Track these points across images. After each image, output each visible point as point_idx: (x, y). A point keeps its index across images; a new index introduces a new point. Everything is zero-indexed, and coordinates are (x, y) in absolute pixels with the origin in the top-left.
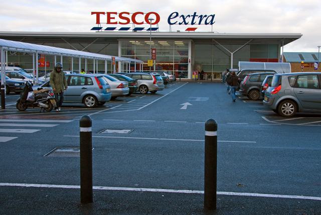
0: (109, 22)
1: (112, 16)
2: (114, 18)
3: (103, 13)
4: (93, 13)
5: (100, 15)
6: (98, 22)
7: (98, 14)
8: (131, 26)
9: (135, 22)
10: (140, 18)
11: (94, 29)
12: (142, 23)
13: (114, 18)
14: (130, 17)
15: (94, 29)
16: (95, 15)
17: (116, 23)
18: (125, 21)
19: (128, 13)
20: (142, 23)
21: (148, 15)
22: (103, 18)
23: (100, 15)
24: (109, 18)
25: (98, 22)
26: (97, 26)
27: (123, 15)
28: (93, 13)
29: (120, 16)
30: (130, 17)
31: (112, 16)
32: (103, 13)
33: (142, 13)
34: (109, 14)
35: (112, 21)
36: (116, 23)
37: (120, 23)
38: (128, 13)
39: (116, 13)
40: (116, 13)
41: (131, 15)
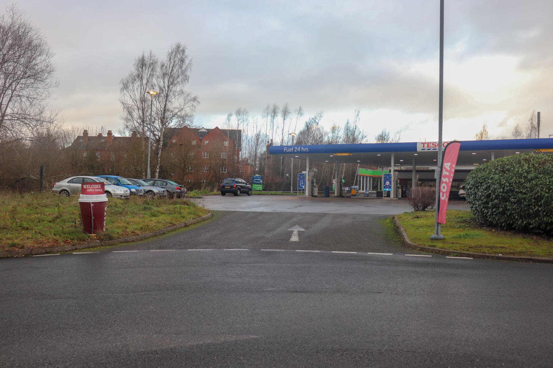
0: (428, 147)
1: (429, 144)
3: (426, 143)
4: (422, 143)
5: (425, 144)
6: (424, 147)
11: (422, 150)
15: (422, 150)
16: (423, 144)
18: (435, 146)
21: (444, 143)
22: (426, 145)
23: (425, 144)
24: (428, 145)
25: (424, 147)
27: (434, 144)
28: (422, 143)
29: (433, 144)
32: (426, 143)
34: (428, 143)
36: (431, 147)
38: (436, 143)
39: (431, 143)
40: (431, 143)
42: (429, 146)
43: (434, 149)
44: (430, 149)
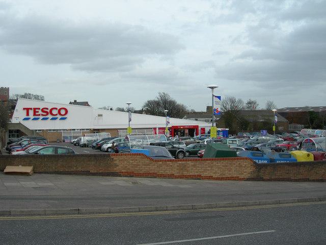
0: (35, 115)
1: (37, 110)
2: (38, 112)
3: (31, 109)
4: (24, 109)
5: (30, 111)
6: (28, 114)
7: (28, 110)
8: (50, 116)
9: (52, 114)
10: (55, 112)
12: (57, 115)
13: (38, 112)
14: (48, 111)
16: (25, 111)
17: (39, 115)
18: (46, 114)
19: (47, 109)
20: (57, 115)
22: (31, 112)
25: (28, 114)
26: (27, 117)
29: (42, 110)
30: (48, 111)
31: (37, 110)
33: (56, 109)
34: (35, 109)
35: (37, 114)
36: (39, 115)
37: (42, 115)
40: (39, 109)
41: (50, 109)
42: (37, 114)
43: (44, 119)
44: (37, 119)
